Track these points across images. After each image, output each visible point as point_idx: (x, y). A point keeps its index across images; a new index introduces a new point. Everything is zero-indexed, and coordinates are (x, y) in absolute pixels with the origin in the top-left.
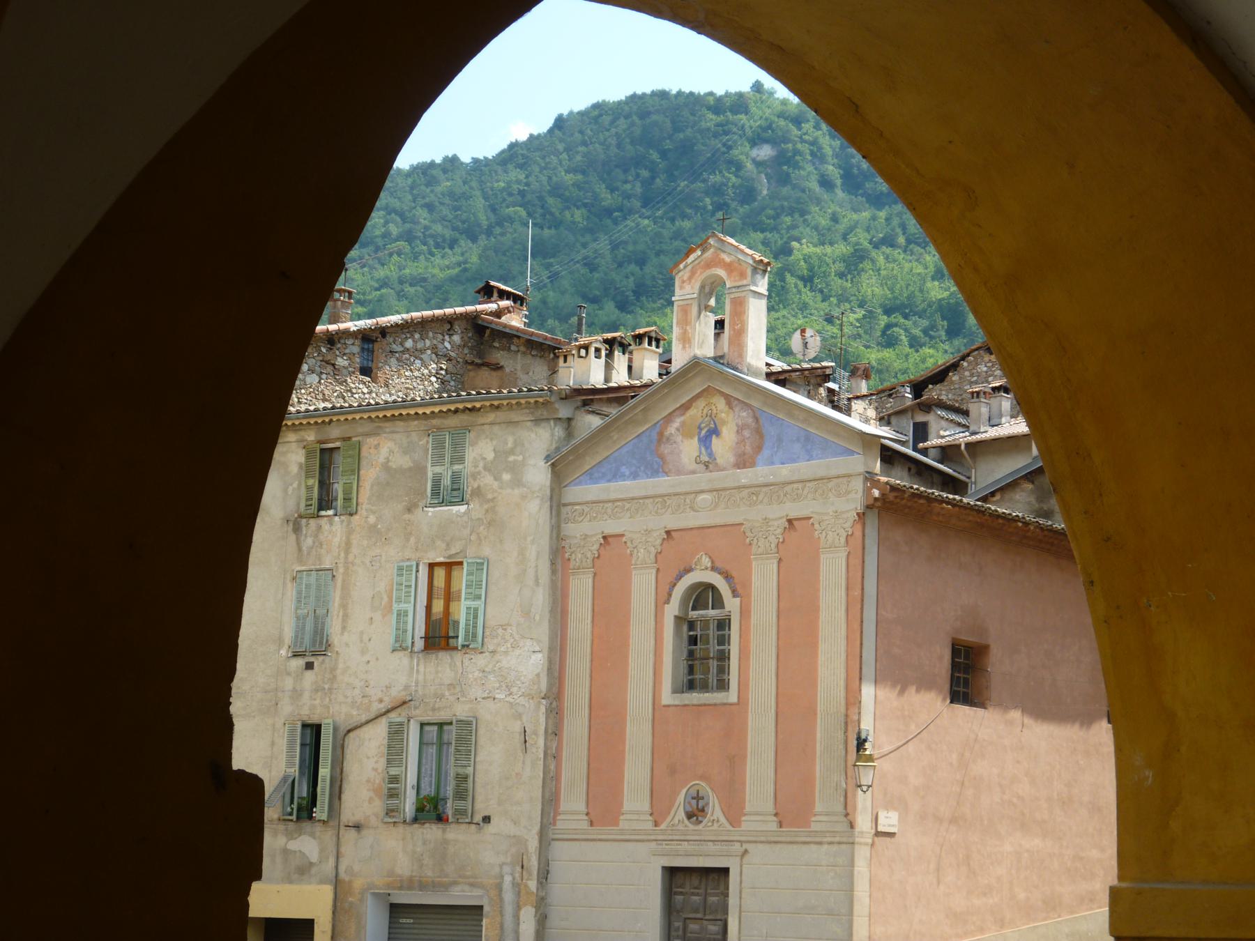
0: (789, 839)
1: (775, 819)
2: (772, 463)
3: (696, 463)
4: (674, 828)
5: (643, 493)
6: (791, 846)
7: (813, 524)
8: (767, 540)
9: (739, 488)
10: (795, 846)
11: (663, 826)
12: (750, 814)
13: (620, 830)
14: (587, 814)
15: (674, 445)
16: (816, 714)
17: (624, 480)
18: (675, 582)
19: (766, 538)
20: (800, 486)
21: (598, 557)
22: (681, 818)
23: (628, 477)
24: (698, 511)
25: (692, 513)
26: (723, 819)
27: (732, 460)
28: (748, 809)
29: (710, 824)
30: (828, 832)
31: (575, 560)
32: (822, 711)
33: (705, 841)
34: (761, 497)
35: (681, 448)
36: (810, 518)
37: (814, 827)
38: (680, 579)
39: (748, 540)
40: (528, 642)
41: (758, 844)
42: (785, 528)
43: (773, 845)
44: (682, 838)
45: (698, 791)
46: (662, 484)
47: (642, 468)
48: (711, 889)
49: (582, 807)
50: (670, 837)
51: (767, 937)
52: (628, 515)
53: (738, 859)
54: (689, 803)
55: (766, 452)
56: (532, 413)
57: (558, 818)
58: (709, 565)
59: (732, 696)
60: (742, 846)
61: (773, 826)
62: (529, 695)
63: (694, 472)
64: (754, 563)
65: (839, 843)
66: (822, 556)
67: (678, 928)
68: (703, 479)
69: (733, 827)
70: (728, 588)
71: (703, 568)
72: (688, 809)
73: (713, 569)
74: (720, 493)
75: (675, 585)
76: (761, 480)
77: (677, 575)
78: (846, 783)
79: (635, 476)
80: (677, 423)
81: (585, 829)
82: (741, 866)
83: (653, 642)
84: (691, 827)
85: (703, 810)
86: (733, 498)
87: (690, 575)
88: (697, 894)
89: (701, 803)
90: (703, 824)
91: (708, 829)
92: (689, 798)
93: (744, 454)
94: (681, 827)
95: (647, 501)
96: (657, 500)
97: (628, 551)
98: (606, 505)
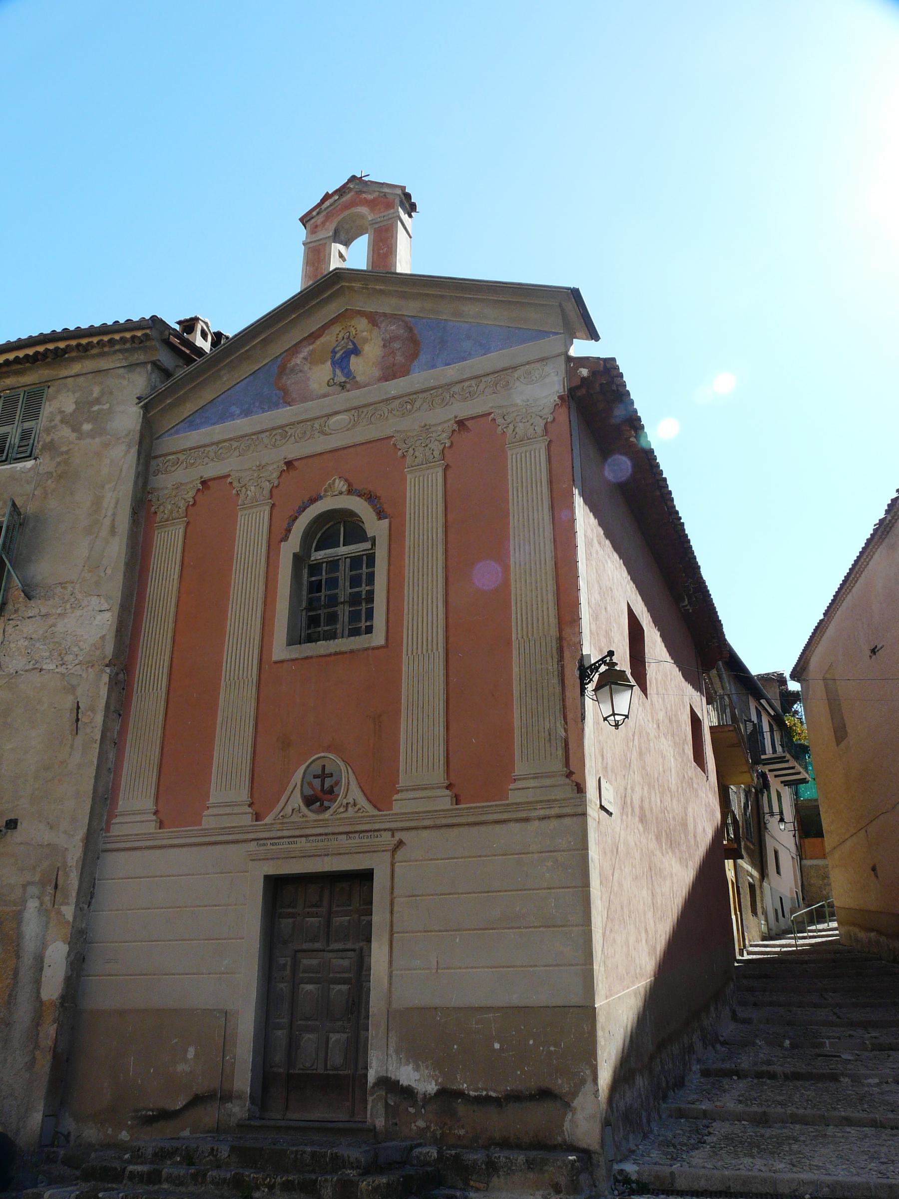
0: (471, 819)
1: (448, 792)
2: (433, 367)
3: (328, 385)
4: (285, 820)
5: (258, 428)
6: (475, 829)
7: (494, 420)
8: (427, 448)
9: (387, 400)
10: (483, 828)
11: (268, 820)
12: (407, 790)
13: (202, 830)
14: (156, 813)
15: (300, 374)
16: (509, 643)
17: (234, 420)
18: (297, 515)
19: (427, 445)
20: (473, 382)
21: (193, 505)
22: (296, 806)
23: (239, 416)
24: (331, 434)
25: (322, 437)
26: (362, 801)
27: (377, 373)
28: (403, 781)
29: (342, 810)
30: (537, 802)
31: (163, 512)
32: (520, 636)
33: (333, 834)
34: (417, 405)
35: (308, 375)
36: (490, 414)
37: (514, 797)
38: (303, 511)
39: (400, 453)
40: (94, 600)
41: (420, 831)
42: (454, 431)
43: (443, 830)
44: (297, 833)
45: (324, 766)
46: (283, 414)
47: (257, 404)
48: (338, 906)
49: (150, 804)
50: (279, 834)
51: (437, 969)
52: (237, 453)
53: (388, 855)
54: (310, 784)
55: (424, 357)
56: (126, 359)
57: (114, 821)
58: (345, 488)
59: (378, 638)
60: (393, 836)
61: (446, 803)
62: (89, 662)
63: (325, 396)
64: (408, 477)
65: (559, 816)
66: (509, 453)
67: (285, 965)
68: (342, 399)
69: (379, 810)
70: (371, 510)
71: (336, 493)
72: (309, 792)
73: (350, 492)
74: (361, 410)
75: (296, 518)
76: (417, 387)
77: (300, 508)
78: (566, 730)
79: (247, 413)
80: (305, 352)
81: (150, 834)
82: (393, 865)
83: (262, 587)
84: (312, 816)
85: (331, 791)
86: (379, 412)
87: (319, 503)
88: (316, 915)
89: (328, 783)
90: (331, 811)
91: (338, 816)
92: (309, 778)
93: (394, 365)
94: (296, 818)
95: (264, 435)
96: (274, 432)
97: (234, 492)
98: (207, 449)
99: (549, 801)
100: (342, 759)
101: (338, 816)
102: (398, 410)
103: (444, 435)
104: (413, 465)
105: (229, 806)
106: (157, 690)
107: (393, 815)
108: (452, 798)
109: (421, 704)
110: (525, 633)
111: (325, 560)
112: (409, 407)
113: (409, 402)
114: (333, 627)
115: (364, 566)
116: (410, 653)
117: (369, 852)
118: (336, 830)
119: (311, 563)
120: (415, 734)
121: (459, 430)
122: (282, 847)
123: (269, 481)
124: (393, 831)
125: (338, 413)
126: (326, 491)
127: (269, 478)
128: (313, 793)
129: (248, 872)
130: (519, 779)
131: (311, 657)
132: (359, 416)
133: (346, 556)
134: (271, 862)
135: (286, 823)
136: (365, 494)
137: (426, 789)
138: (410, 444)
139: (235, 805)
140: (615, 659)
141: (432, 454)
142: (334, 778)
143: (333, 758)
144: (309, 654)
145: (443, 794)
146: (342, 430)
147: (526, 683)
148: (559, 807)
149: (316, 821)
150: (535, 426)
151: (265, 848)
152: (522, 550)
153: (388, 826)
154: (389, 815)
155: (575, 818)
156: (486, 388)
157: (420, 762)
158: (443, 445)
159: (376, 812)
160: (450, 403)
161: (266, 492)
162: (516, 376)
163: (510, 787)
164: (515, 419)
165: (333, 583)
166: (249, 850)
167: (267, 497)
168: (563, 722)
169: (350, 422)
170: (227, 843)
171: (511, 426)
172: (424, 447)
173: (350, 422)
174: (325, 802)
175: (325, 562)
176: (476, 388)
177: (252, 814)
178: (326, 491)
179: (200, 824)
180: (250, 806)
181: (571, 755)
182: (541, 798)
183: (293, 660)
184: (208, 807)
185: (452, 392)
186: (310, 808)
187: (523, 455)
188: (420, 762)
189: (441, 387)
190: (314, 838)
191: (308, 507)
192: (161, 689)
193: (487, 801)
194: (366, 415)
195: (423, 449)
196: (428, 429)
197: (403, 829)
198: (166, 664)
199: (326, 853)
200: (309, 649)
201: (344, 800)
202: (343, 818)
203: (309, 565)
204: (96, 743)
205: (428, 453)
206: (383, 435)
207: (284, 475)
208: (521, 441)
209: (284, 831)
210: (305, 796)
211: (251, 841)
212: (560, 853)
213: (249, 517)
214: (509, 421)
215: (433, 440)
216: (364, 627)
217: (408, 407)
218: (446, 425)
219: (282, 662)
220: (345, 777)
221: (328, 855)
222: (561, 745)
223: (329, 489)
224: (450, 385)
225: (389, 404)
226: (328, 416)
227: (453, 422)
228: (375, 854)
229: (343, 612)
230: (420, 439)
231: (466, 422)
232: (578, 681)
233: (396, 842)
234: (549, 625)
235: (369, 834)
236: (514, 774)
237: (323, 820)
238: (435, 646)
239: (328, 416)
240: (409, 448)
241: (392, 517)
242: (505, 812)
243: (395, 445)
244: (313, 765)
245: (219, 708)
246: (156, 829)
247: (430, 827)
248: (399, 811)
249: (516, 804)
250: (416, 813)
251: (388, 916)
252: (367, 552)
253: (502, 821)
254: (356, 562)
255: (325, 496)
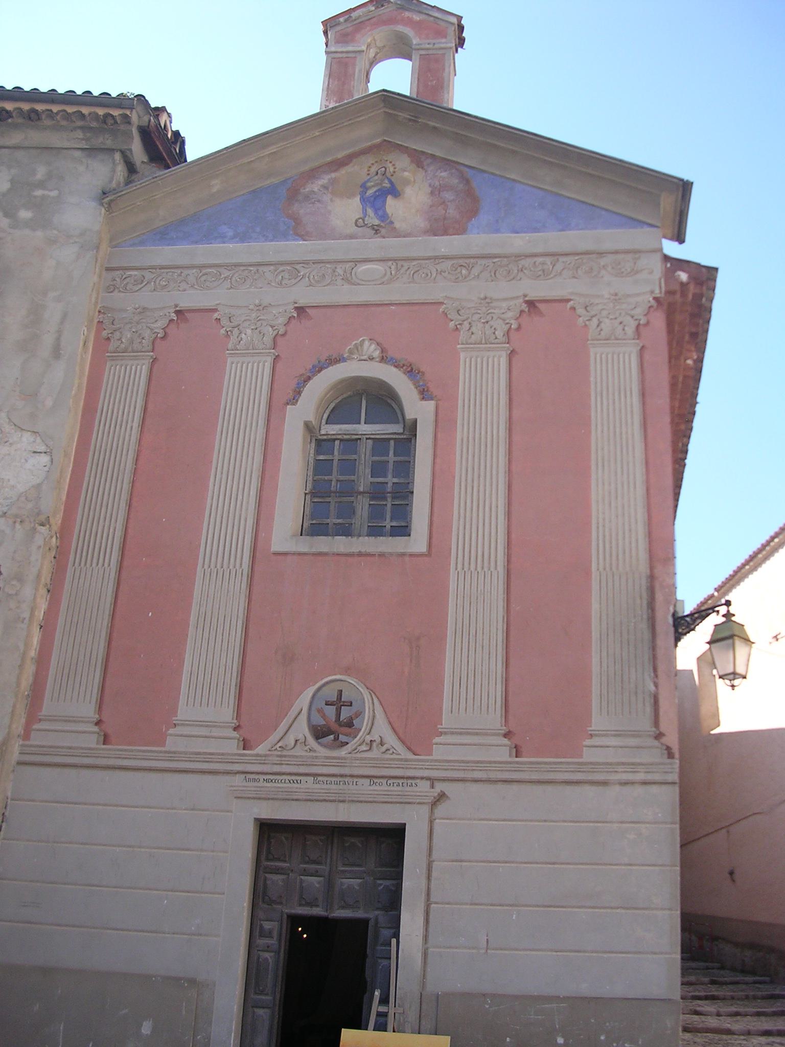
0: (535, 776)
1: (506, 741)
2: (497, 231)
3: (356, 225)
4: (285, 753)
5: (257, 259)
6: (541, 788)
7: (573, 309)
8: (487, 326)
9: (436, 258)
10: (549, 788)
11: (261, 749)
12: (452, 733)
13: (166, 752)
14: (98, 723)
15: (318, 205)
16: (588, 573)
17: (224, 243)
18: (310, 374)
19: (487, 322)
20: (548, 260)
21: (163, 338)
22: (301, 737)
23: (232, 238)
24: (359, 284)
25: (346, 286)
26: (391, 740)
27: (422, 224)
28: (446, 721)
29: (364, 748)
30: (618, 764)
31: (120, 339)
32: (601, 569)
33: (352, 776)
34: (475, 271)
35: (329, 208)
36: (568, 300)
37: (589, 756)
38: (319, 371)
39: (452, 324)
40: (27, 437)
41: (468, 784)
42: (522, 312)
43: (500, 786)
44: (302, 770)
45: (340, 692)
46: (295, 249)
47: (258, 230)
48: (344, 865)
49: (88, 710)
50: (277, 769)
51: (487, 949)
52: (227, 284)
53: (426, 809)
54: (320, 711)
55: (484, 217)
56: (87, 140)
57: (35, 727)
58: (377, 354)
59: (418, 542)
60: (432, 787)
61: (502, 752)
62: (16, 516)
63: (352, 237)
64: (462, 355)
65: (645, 783)
66: (592, 351)
67: (271, 931)
68: (375, 245)
69: (415, 754)
70: (412, 387)
71: (365, 357)
72: (318, 720)
73: (383, 359)
74: (400, 263)
75: (309, 378)
76: (475, 251)
77: (314, 367)
78: (656, 685)
79: (243, 237)
80: (324, 180)
81: (90, 749)
82: (431, 822)
83: (258, 457)
84: (322, 752)
85: (350, 724)
86: (425, 271)
87: (340, 367)
88: (316, 874)
89: (345, 713)
90: (349, 747)
91: (358, 755)
92: (321, 704)
93: (445, 219)
94: (299, 751)
95: (265, 269)
96: (281, 268)
97: (223, 331)
98: (186, 272)
99: (633, 764)
100: (365, 685)
101: (358, 755)
102: (449, 273)
103: (510, 314)
104: (469, 341)
105: (207, 726)
106: (103, 565)
107: (432, 761)
108: (511, 748)
109: (473, 632)
110: (607, 565)
111: (339, 437)
112: (464, 272)
113: (465, 267)
114: (348, 521)
115: (391, 453)
116: (460, 566)
117: (401, 803)
118: (356, 772)
119: (320, 437)
120: (464, 667)
121: (529, 311)
122: (281, 785)
123: (272, 327)
124: (432, 781)
125: (370, 261)
126: (351, 352)
127: (273, 323)
128: (324, 723)
129: (231, 812)
130: (596, 735)
131: (326, 554)
132: (397, 270)
133: (368, 436)
134: (264, 803)
135: (285, 756)
136: (404, 365)
137: (477, 734)
138: (465, 317)
139: (215, 726)
140: (732, 609)
141: (494, 333)
142: (354, 709)
143: (353, 682)
144: (325, 549)
145: (500, 742)
146: (374, 283)
147: (607, 624)
148: (645, 772)
149: (327, 758)
150: (625, 326)
151: (256, 784)
152: (606, 468)
153: (426, 773)
154: (427, 761)
155: (664, 787)
156: (563, 269)
157: (470, 702)
158: (508, 326)
159: (410, 756)
160: (519, 278)
161: (268, 340)
162: (602, 264)
163: (585, 743)
164: (600, 313)
165: (349, 467)
166: (233, 784)
167: (268, 346)
168: (652, 674)
169: (385, 274)
170: (201, 772)
171: (595, 320)
172: (484, 323)
173: (385, 274)
174: (340, 736)
175: (338, 439)
176: (551, 267)
177: (238, 740)
178: (351, 352)
179: (164, 745)
180: (235, 729)
181: (661, 713)
182: (623, 760)
183: (300, 554)
184: (175, 725)
185: (520, 266)
186: (319, 740)
187: (610, 356)
188: (470, 702)
189: (509, 257)
190: (325, 779)
191: (326, 368)
192: (109, 565)
193: (557, 756)
194: (406, 271)
195: (482, 325)
196: (488, 303)
197: (444, 780)
198: (119, 534)
199: (341, 799)
200: (323, 544)
201: (368, 736)
202: (365, 759)
203: (316, 440)
204: (23, 622)
205: (489, 332)
206: (431, 298)
207: (293, 322)
208: (607, 340)
209: (284, 766)
210: (313, 726)
211: (236, 773)
212: (643, 826)
213: (242, 367)
214: (593, 313)
215: (495, 317)
216: (388, 527)
217: (464, 272)
218: (512, 303)
219: (285, 554)
220: (369, 708)
221: (343, 801)
222: (649, 702)
223: (356, 351)
224: (519, 257)
225: (438, 263)
226: (357, 262)
227: (521, 300)
228: (407, 806)
229: (363, 506)
230: (479, 313)
231: (537, 304)
232: (672, 629)
233: (436, 794)
234: (638, 560)
235: (401, 781)
236: (590, 729)
237: (339, 758)
238: (493, 564)
239: (357, 262)
240: (464, 321)
241: (440, 400)
242: (579, 771)
243: (445, 314)
244: (324, 689)
245: (194, 601)
246: (97, 744)
247: (481, 781)
248: (439, 758)
249: (591, 763)
250: (463, 762)
251: (424, 882)
252: (397, 436)
253: (573, 782)
254: (380, 444)
255: (350, 358)
